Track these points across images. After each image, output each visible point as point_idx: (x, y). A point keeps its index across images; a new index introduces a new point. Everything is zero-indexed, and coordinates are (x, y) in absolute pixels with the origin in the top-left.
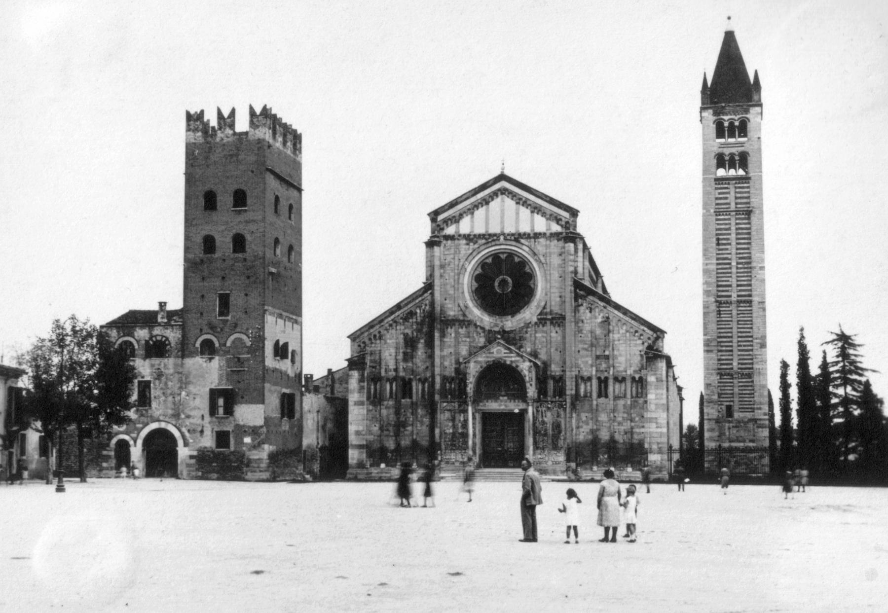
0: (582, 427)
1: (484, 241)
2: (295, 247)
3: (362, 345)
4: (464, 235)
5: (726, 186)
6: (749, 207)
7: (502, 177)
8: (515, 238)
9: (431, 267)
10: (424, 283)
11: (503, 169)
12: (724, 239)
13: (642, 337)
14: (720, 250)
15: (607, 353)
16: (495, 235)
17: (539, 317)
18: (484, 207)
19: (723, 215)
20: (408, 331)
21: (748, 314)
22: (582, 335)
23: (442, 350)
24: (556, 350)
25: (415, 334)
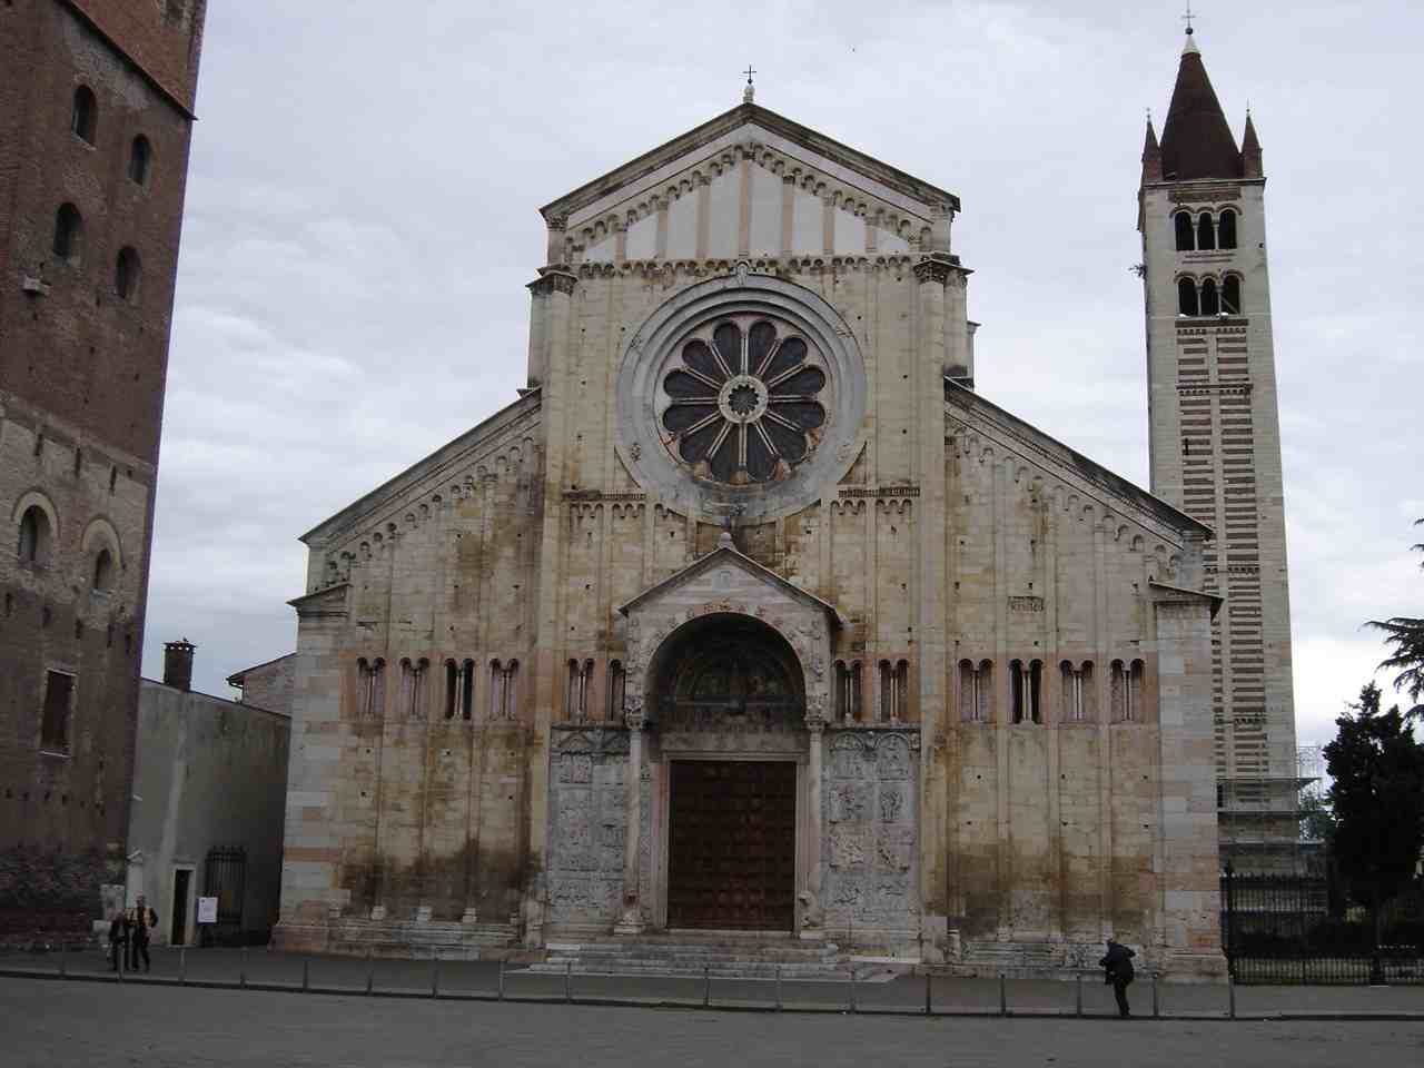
0: (965, 807)
1: (691, 280)
2: (149, 264)
3: (342, 564)
4: (639, 264)
5: (1202, 337)
6: (1247, 379)
7: (749, 112)
8: (778, 271)
9: (540, 347)
10: (520, 392)
11: (750, 93)
12: (1201, 442)
13: (1139, 546)
14: (1189, 463)
15: (1036, 592)
16: (723, 263)
17: (845, 487)
18: (695, 192)
19: (1194, 394)
20: (472, 526)
21: (1250, 594)
22: (968, 540)
23: (562, 577)
24: (893, 580)
25: (489, 534)
